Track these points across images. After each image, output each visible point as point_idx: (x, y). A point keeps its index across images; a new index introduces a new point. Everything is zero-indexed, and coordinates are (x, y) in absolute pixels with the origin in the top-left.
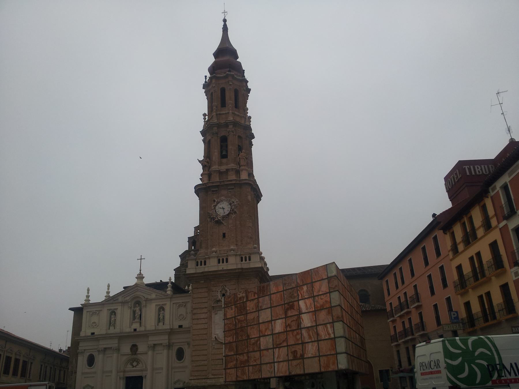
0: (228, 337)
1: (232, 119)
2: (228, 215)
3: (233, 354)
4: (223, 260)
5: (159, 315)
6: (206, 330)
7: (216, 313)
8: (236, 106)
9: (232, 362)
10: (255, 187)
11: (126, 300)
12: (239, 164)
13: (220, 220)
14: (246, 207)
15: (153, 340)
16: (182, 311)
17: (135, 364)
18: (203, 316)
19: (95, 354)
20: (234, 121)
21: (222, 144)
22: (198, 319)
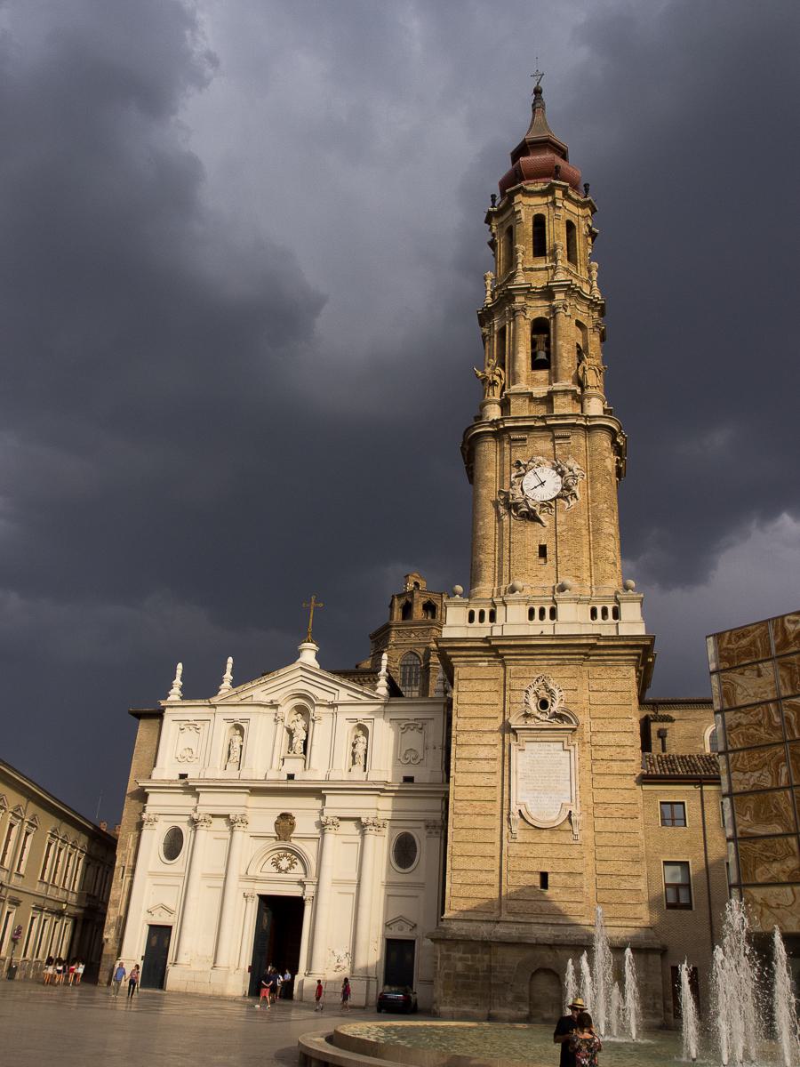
0: (745, 773)
1: (564, 279)
2: (554, 499)
3: (779, 830)
4: (542, 611)
5: (354, 745)
6: (492, 789)
7: (521, 748)
8: (572, 257)
9: (775, 860)
10: (618, 440)
11: (272, 702)
12: (580, 382)
13: (534, 511)
14: (602, 485)
15: (337, 804)
16: (414, 739)
17: (284, 863)
18: (484, 752)
19: (186, 830)
20: (569, 283)
21: (535, 336)
22: (468, 759)
